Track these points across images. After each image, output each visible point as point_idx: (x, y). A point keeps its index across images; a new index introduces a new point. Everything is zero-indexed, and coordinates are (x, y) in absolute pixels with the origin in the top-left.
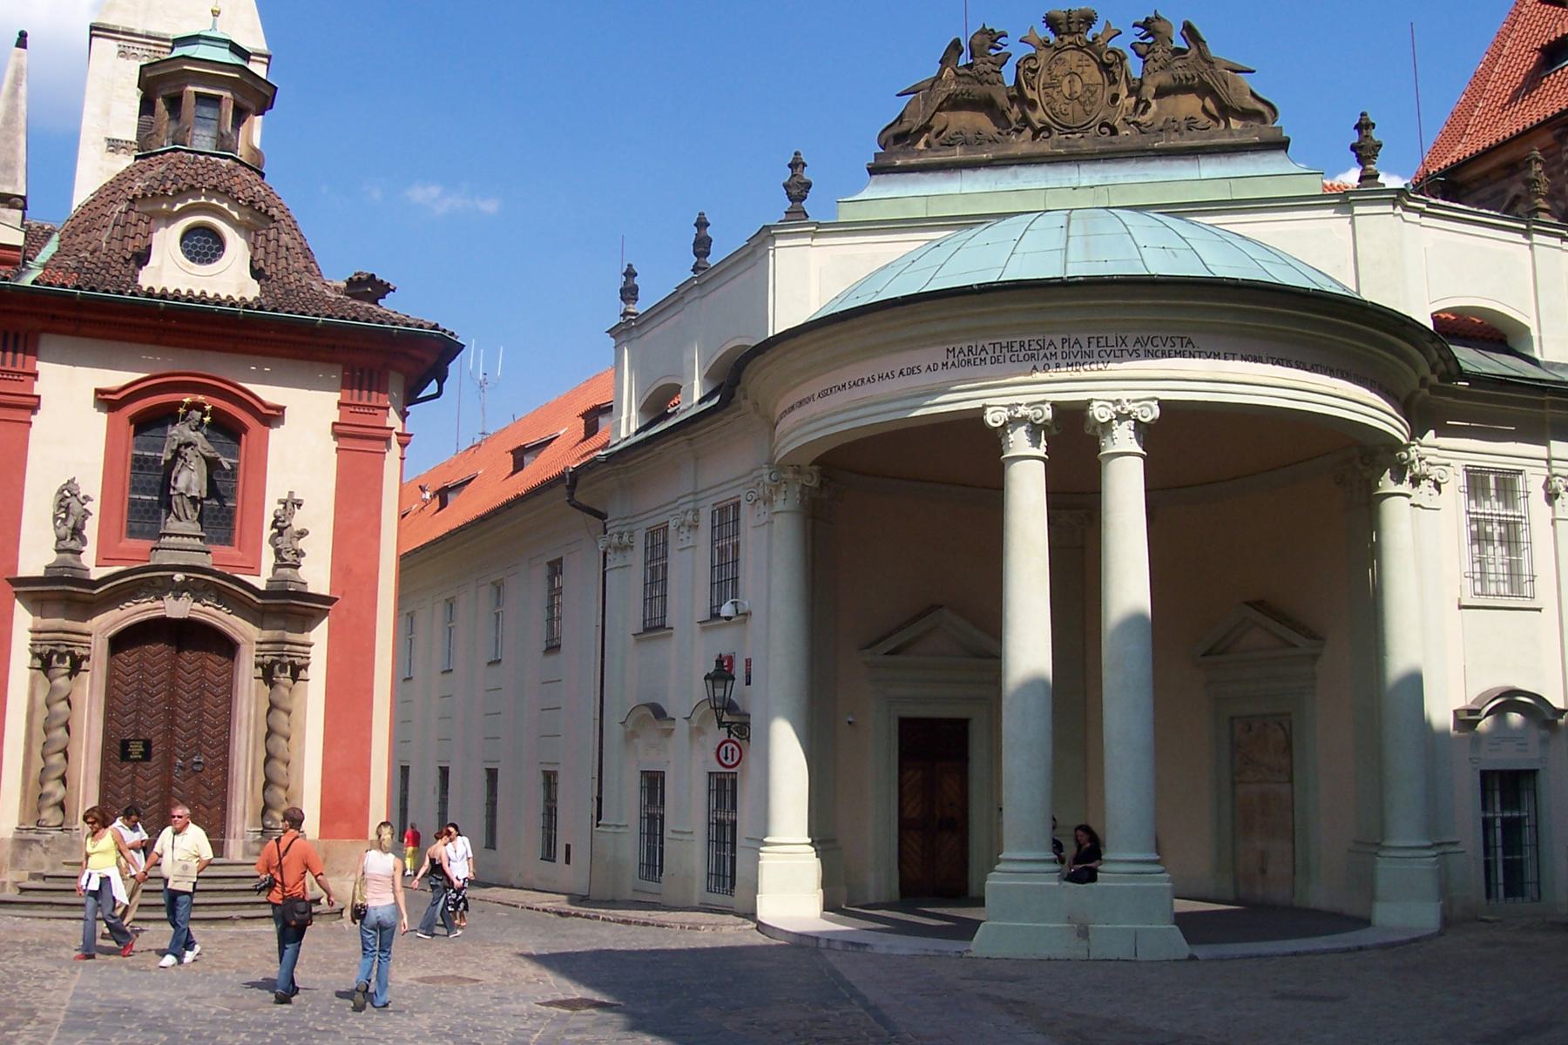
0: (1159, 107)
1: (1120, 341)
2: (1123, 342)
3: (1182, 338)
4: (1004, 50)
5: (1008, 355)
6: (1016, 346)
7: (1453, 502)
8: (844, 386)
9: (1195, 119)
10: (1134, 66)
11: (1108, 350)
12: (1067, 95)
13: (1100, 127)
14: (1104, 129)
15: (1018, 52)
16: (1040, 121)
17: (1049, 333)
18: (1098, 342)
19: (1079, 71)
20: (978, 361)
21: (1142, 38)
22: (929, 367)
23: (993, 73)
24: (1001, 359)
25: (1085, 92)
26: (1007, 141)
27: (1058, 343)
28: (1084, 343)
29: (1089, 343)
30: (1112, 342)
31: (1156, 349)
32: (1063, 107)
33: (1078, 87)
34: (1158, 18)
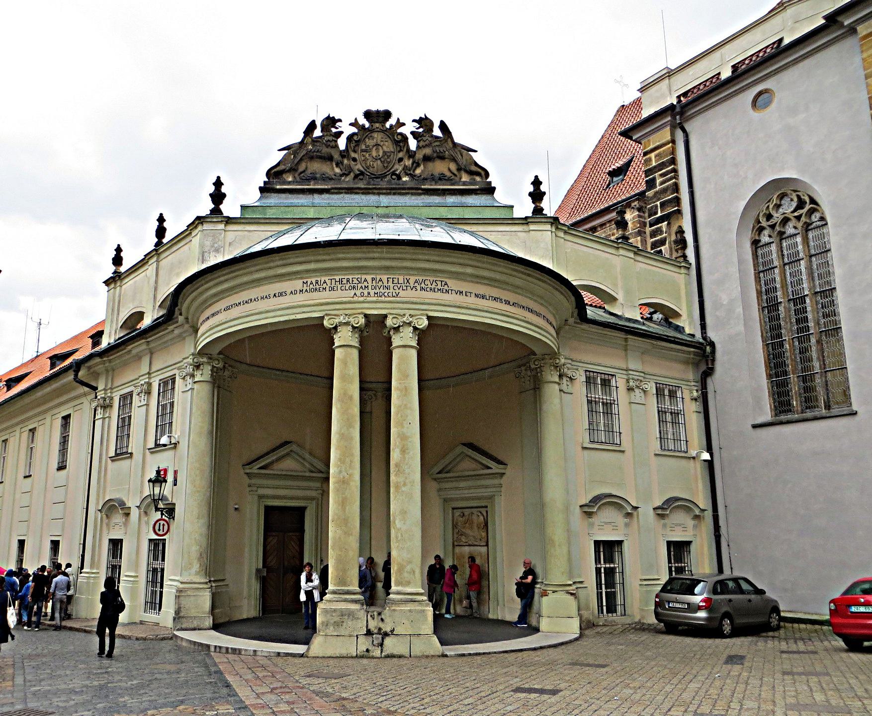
0: (425, 167)
1: (406, 281)
2: (408, 281)
3: (442, 281)
5: (339, 286)
6: (345, 281)
7: (579, 388)
8: (240, 304)
10: (413, 144)
11: (399, 285)
13: (391, 177)
14: (394, 177)
15: (348, 130)
16: (359, 170)
17: (364, 274)
18: (393, 281)
19: (382, 143)
20: (321, 289)
21: (417, 129)
22: (292, 292)
24: (335, 288)
26: (340, 179)
27: (369, 280)
28: (385, 281)
29: (388, 281)
30: (401, 281)
31: (426, 287)
32: (371, 163)
33: (381, 153)
34: (426, 118)
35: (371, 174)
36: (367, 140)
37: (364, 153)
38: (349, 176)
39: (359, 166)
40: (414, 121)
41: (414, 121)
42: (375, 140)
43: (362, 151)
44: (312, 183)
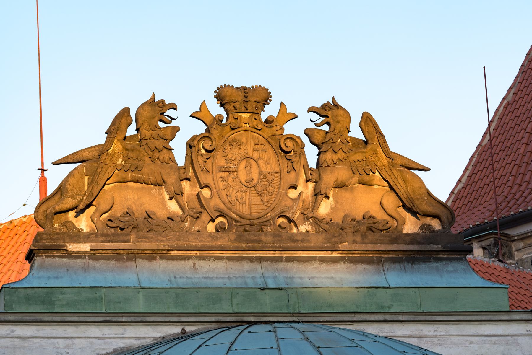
0: (336, 202)
4: (173, 123)
9: (375, 218)
12: (243, 181)
19: (256, 155)
23: (165, 151)
25: (262, 180)
26: (182, 229)
33: (255, 175)
34: (336, 105)
35: (241, 217)
36: (228, 148)
37: (225, 175)
38: (199, 221)
39: (216, 202)
40: (312, 110)
41: (312, 110)
42: (243, 148)
43: (221, 169)
44: (132, 237)
